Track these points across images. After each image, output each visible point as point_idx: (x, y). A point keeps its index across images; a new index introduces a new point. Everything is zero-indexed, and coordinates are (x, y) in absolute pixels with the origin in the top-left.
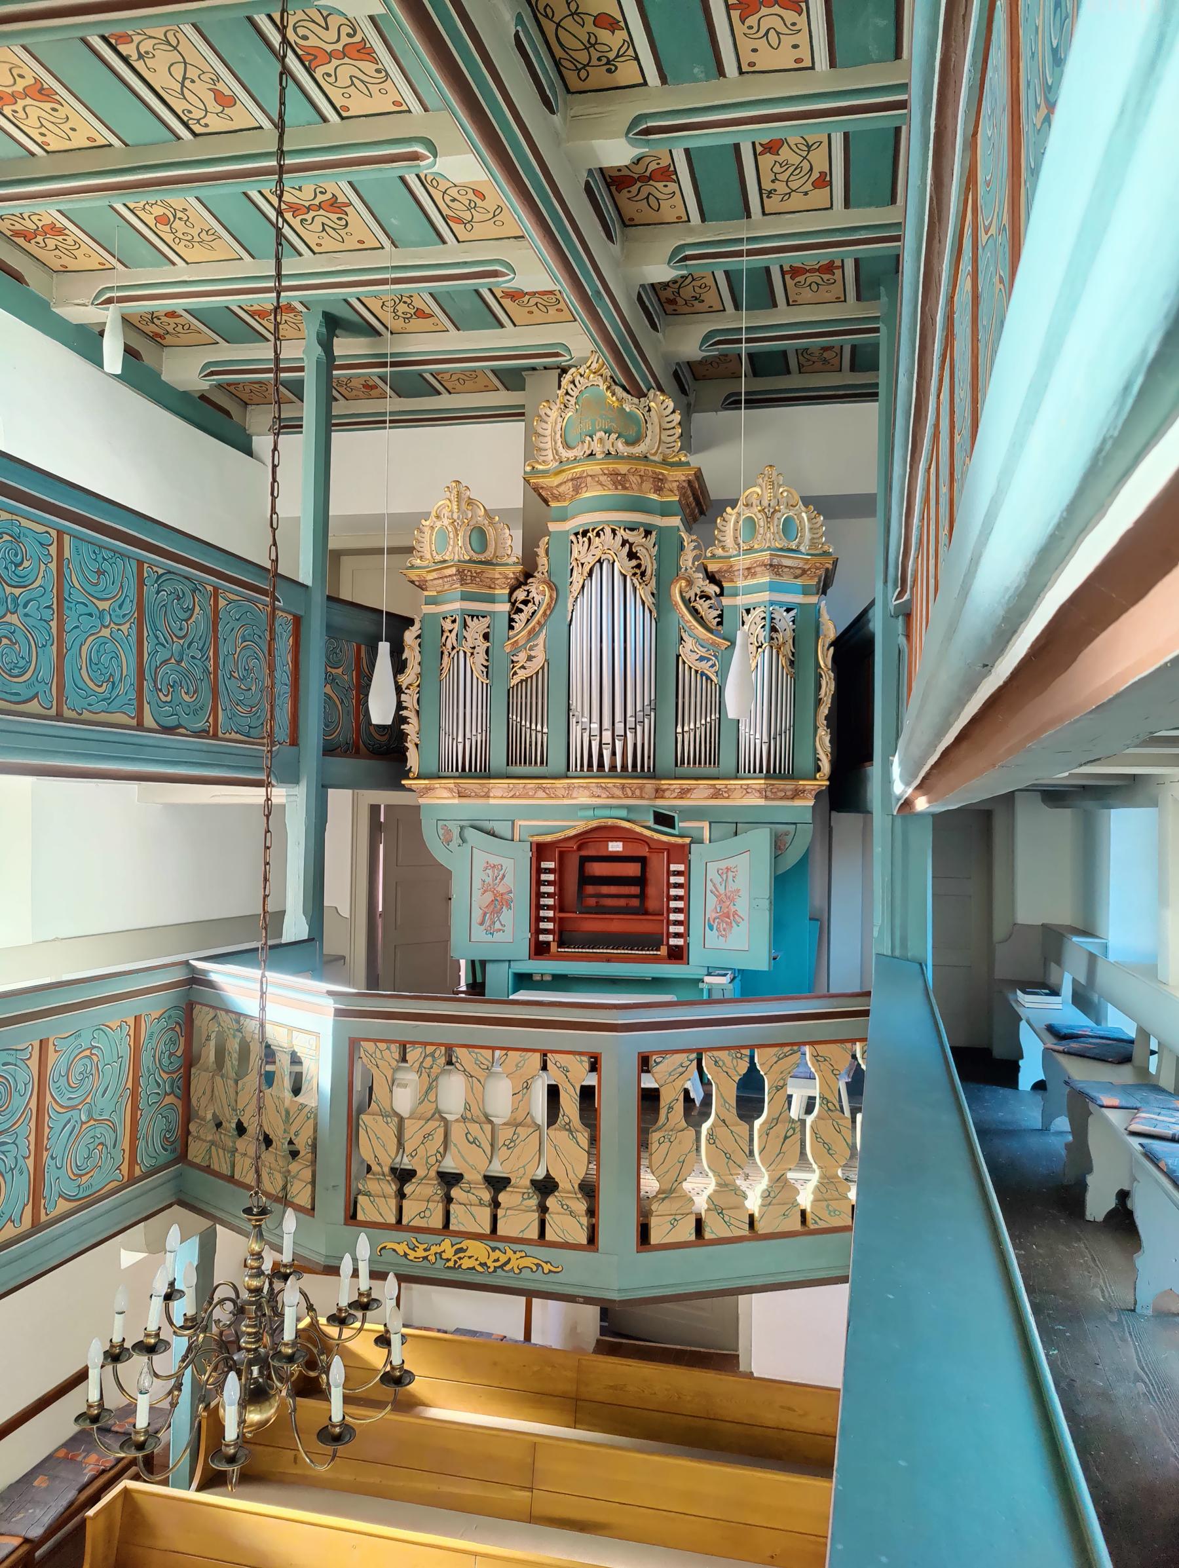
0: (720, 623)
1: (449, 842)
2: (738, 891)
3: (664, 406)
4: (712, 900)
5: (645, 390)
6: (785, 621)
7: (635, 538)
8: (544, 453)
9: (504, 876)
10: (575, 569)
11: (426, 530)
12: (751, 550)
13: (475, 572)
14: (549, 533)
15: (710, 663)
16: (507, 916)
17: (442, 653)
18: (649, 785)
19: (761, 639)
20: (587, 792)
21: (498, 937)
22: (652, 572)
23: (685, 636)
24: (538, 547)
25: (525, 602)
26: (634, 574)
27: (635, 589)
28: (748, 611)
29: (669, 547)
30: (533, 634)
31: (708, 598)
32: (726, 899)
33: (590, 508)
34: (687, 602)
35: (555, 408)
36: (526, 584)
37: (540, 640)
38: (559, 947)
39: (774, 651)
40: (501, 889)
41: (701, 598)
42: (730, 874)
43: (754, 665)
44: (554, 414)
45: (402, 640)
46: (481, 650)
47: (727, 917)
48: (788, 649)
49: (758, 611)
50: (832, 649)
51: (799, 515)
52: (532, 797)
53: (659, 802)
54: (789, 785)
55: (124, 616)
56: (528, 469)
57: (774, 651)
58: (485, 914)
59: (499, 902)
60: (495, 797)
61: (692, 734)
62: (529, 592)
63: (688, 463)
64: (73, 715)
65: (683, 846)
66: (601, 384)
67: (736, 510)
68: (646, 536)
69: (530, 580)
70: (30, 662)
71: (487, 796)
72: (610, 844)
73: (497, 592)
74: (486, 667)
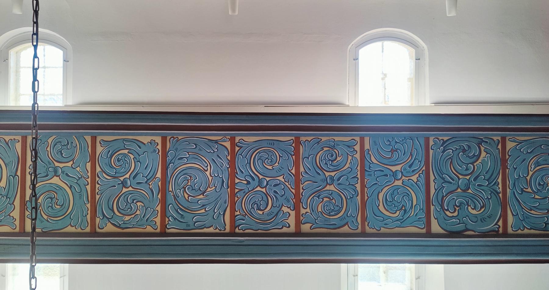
55: (413, 171)
64: (374, 231)
70: (342, 207)
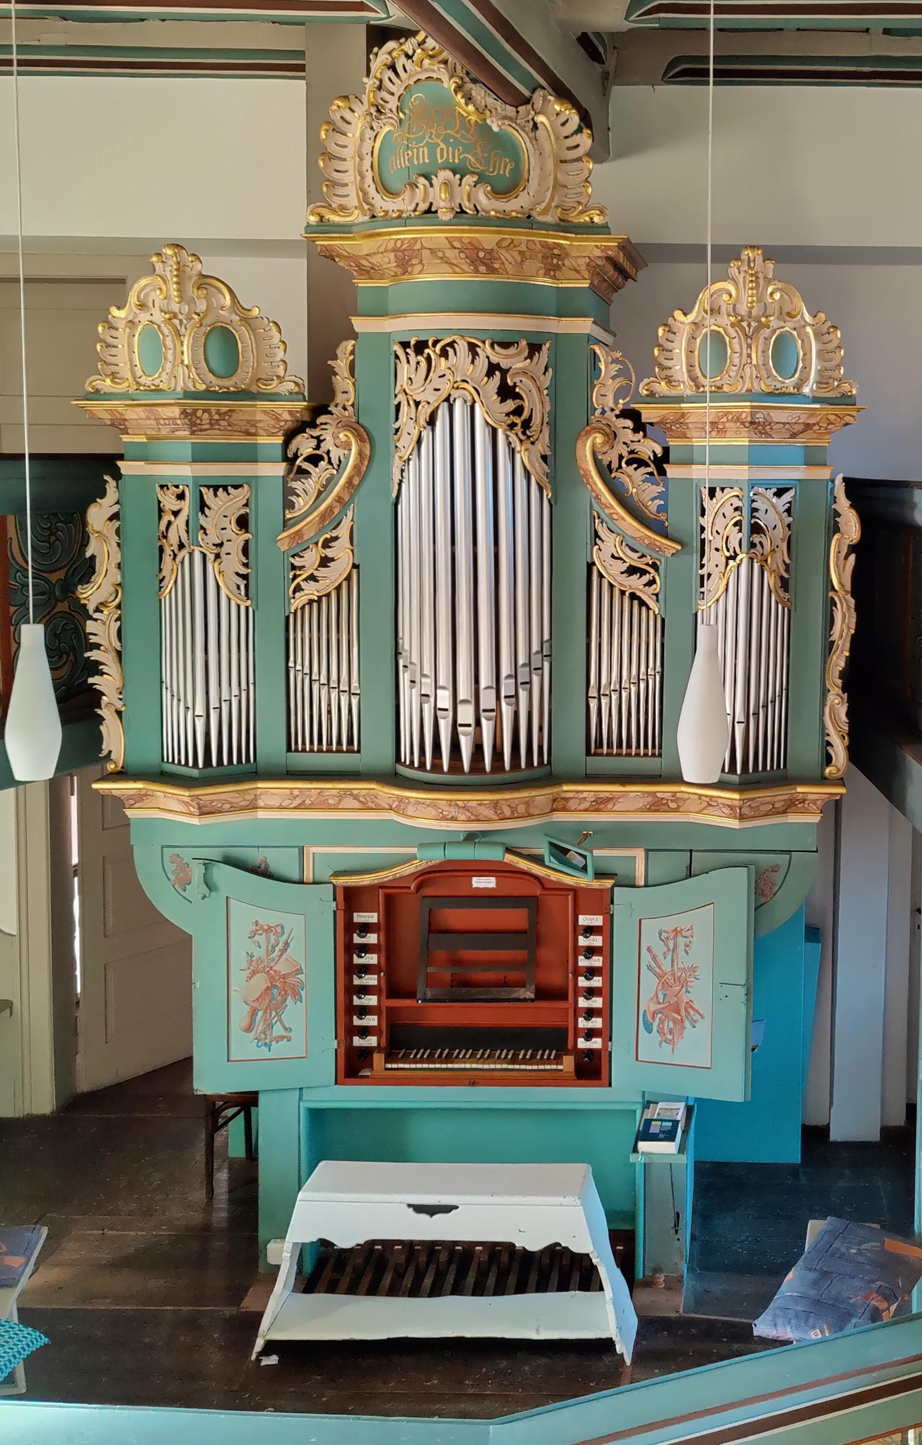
0: (660, 509)
1: (184, 882)
2: (694, 969)
3: (562, 119)
4: (650, 983)
5: (527, 93)
7: (515, 361)
8: (341, 191)
9: (287, 944)
10: (404, 408)
11: (121, 325)
12: (718, 393)
13: (217, 409)
14: (354, 336)
15: (646, 578)
16: (294, 1013)
17: (161, 550)
18: (541, 796)
19: (734, 543)
20: (432, 812)
21: (278, 1049)
22: (543, 410)
23: (602, 531)
24: (335, 358)
25: (314, 460)
26: (512, 426)
27: (512, 452)
28: (712, 493)
29: (571, 369)
30: (331, 519)
31: (641, 463)
32: (674, 982)
33: (423, 297)
34: (605, 471)
35: (360, 109)
36: (314, 425)
37: (343, 531)
38: (386, 1062)
39: (756, 566)
40: (282, 967)
41: (629, 463)
42: (681, 941)
43: (722, 588)
44: (358, 121)
45: (84, 523)
46: (234, 547)
47: (676, 1012)
49: (729, 493)
51: (800, 329)
52: (335, 808)
53: (559, 817)
54: (780, 795)
56: (313, 219)
57: (756, 566)
58: (254, 1013)
59: (280, 990)
60: (265, 808)
61: (614, 697)
62: (319, 441)
63: (604, 229)
65: (600, 891)
66: (445, 77)
67: (691, 317)
68: (530, 356)
69: (322, 419)
71: (253, 806)
72: (474, 879)
73: (261, 440)
74: (245, 577)
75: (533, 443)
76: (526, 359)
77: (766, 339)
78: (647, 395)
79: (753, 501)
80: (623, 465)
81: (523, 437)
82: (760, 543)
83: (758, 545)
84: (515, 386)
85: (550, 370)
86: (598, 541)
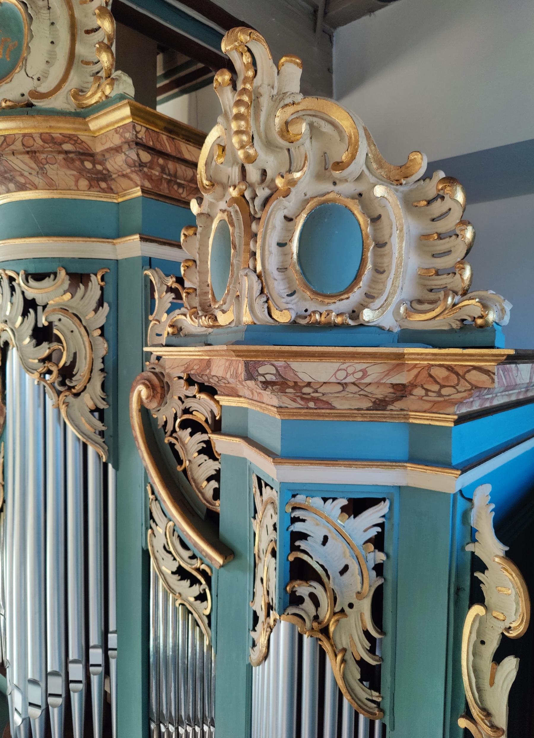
0: (216, 494)
6: (339, 544)
15: (196, 590)
48: (353, 632)
50: (511, 665)
75: (77, 395)
76: (65, 292)
77: (288, 219)
78: (173, 334)
79: (295, 520)
80: (177, 429)
81: (60, 388)
82: (313, 597)
83: (307, 599)
84: (51, 323)
85: (106, 305)
86: (153, 525)
